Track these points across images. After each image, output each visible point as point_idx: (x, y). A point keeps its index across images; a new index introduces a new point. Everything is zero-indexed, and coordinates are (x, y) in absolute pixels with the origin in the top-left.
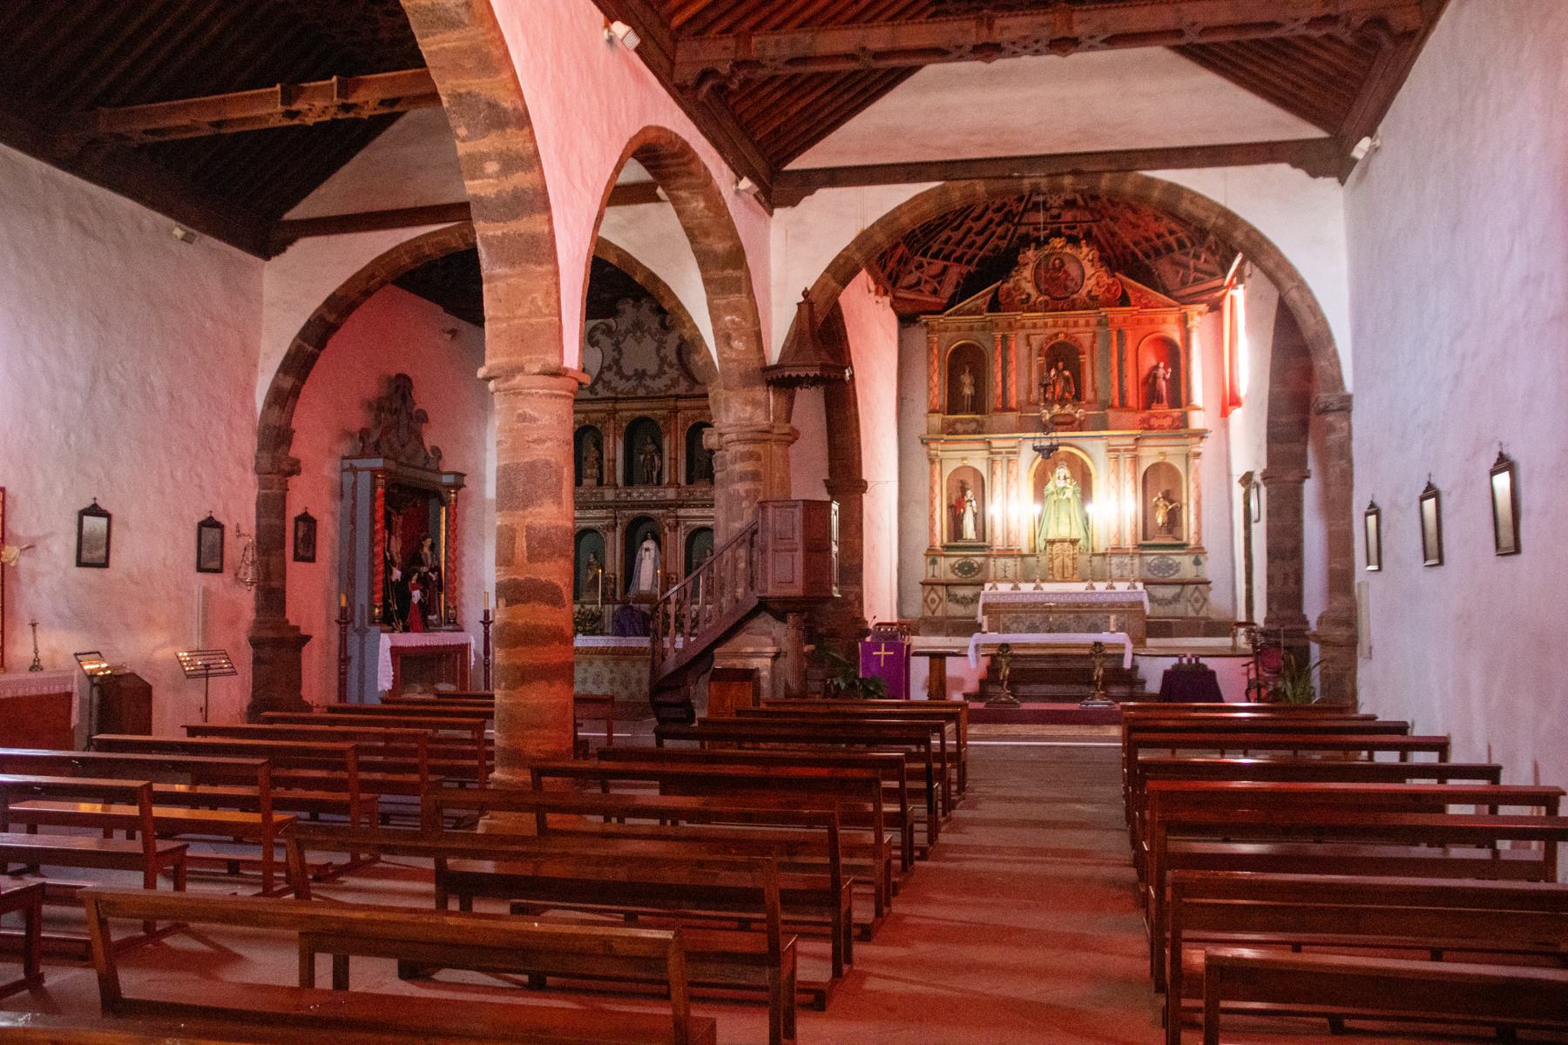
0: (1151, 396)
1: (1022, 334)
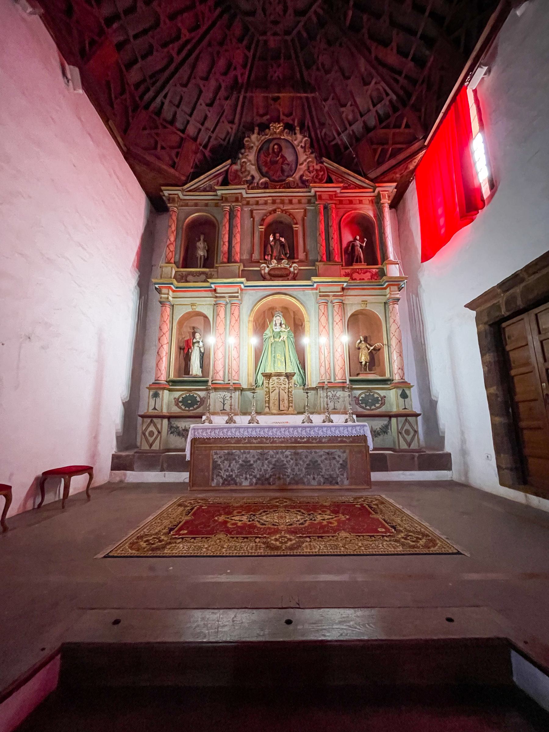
1: (247, 209)
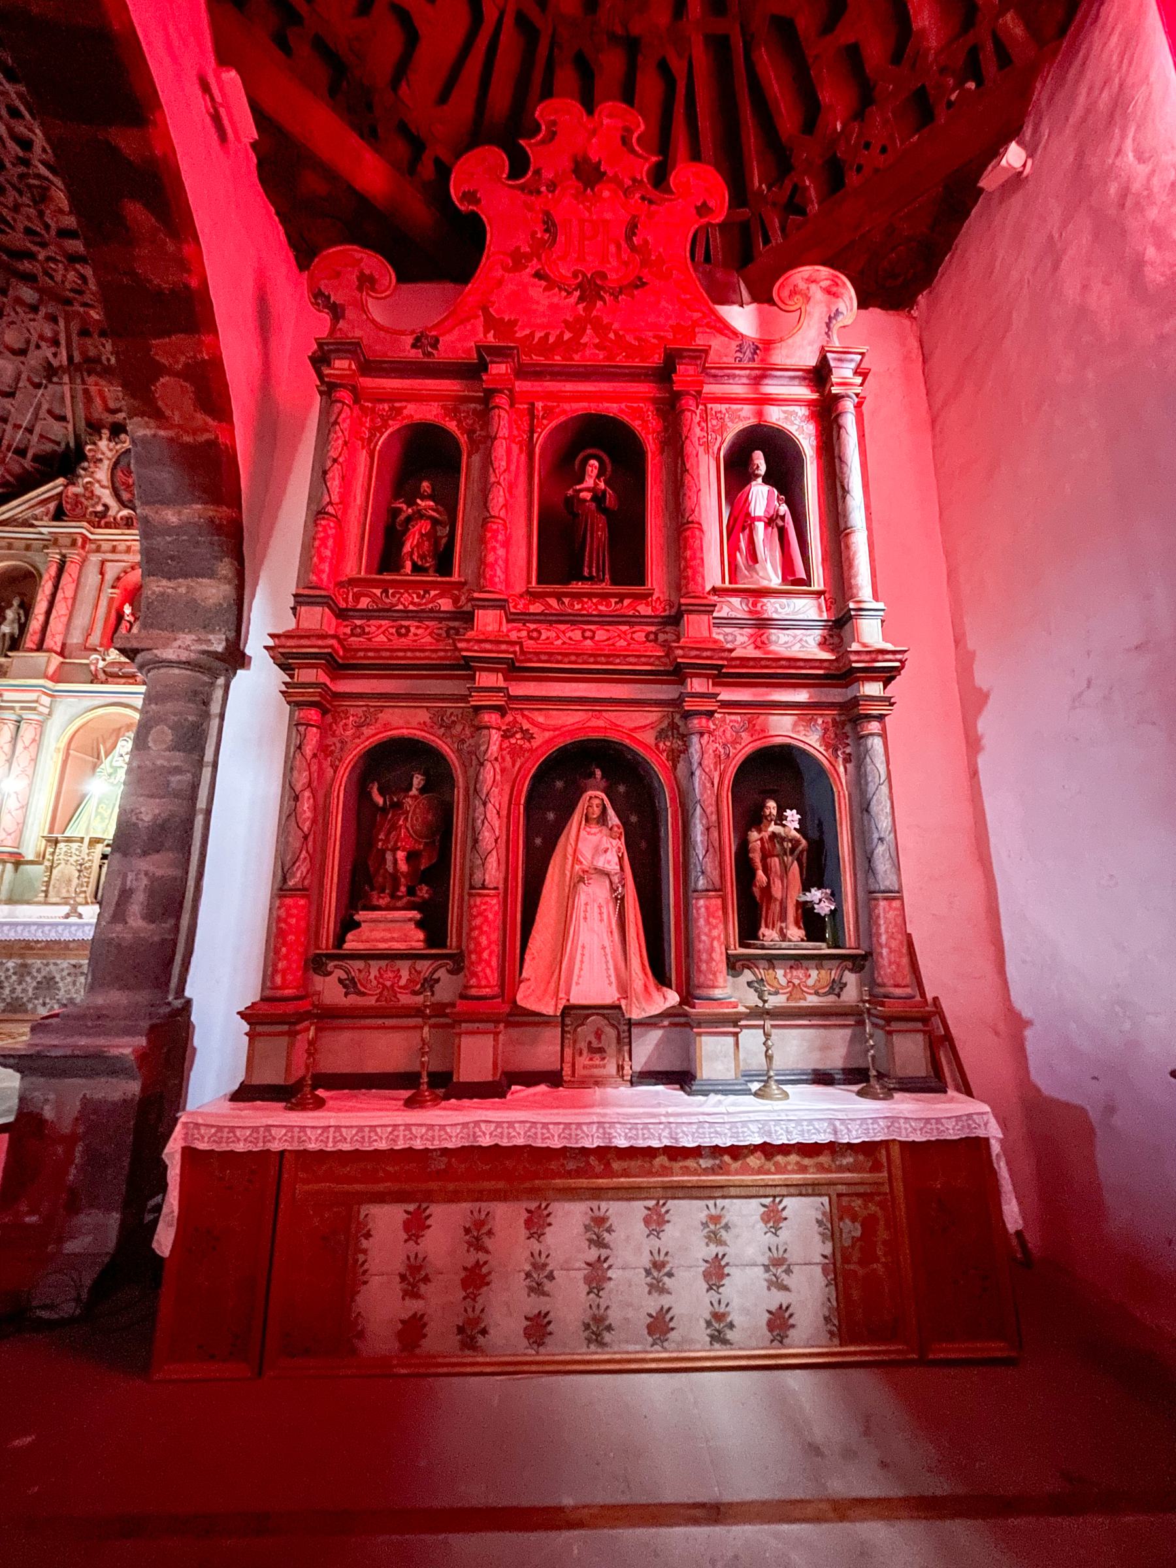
1: (95, 558)
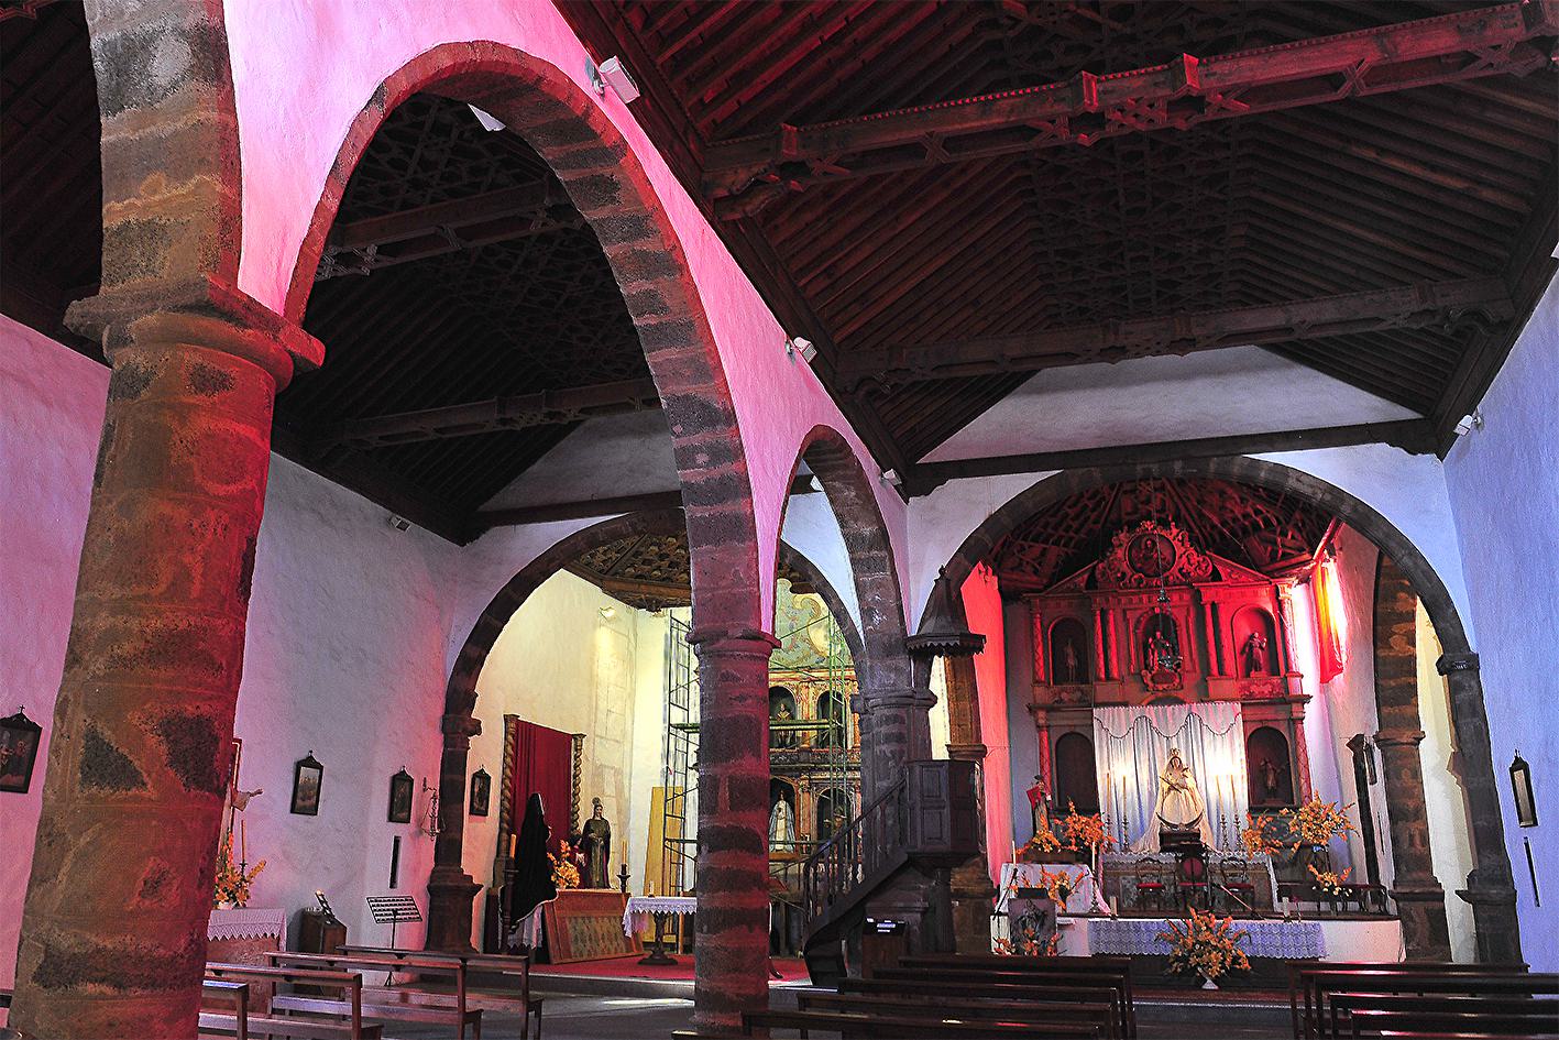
0: (1251, 665)
